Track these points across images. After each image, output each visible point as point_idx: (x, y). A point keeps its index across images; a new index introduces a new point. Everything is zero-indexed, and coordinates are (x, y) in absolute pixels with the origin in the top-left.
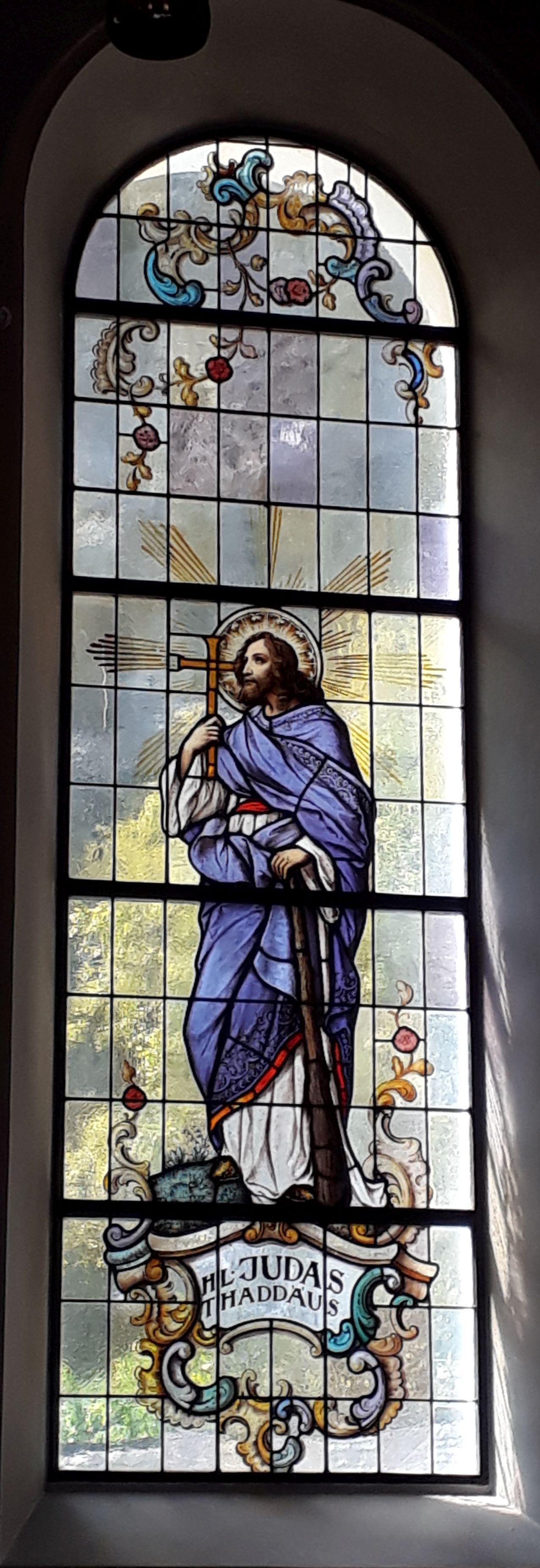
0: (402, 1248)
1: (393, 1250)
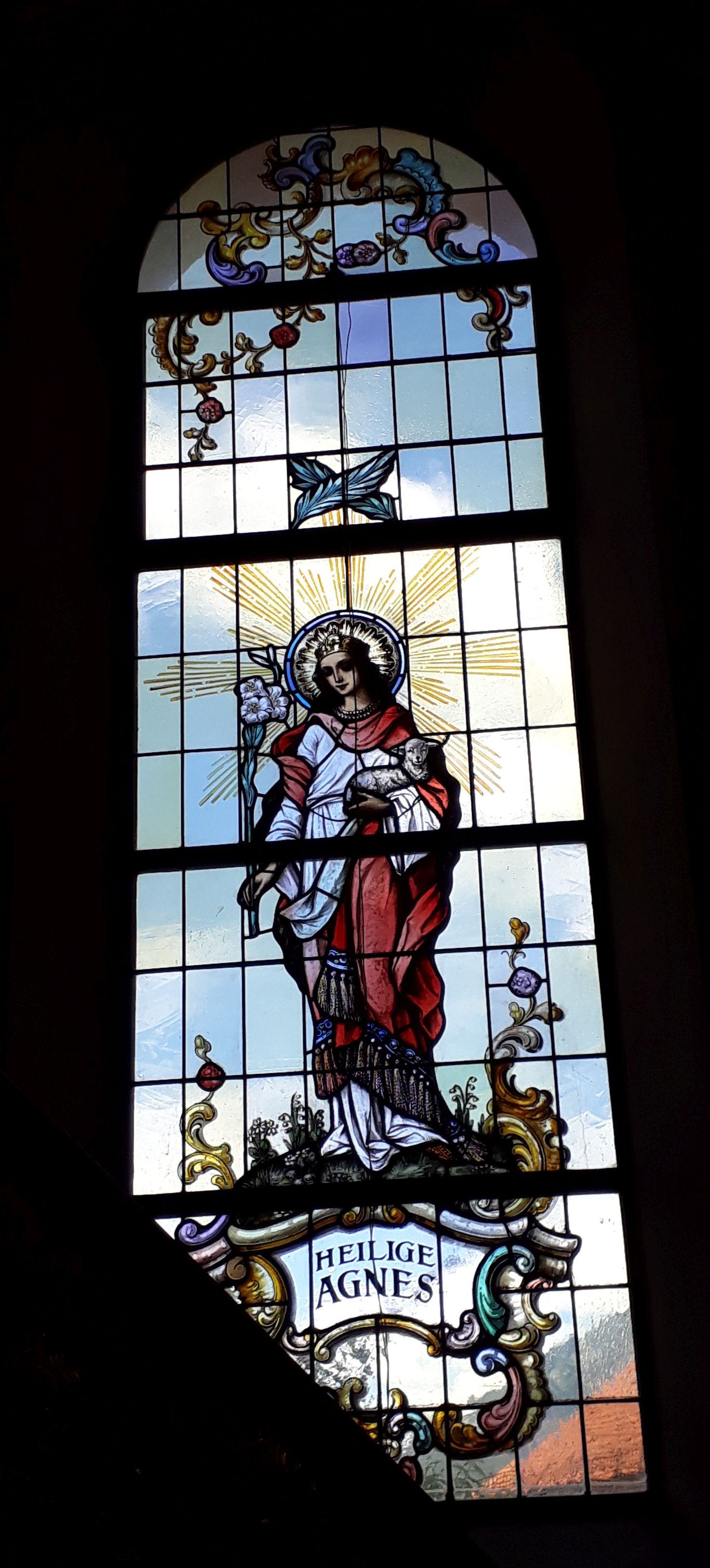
0: (534, 1224)
1: (523, 1223)
